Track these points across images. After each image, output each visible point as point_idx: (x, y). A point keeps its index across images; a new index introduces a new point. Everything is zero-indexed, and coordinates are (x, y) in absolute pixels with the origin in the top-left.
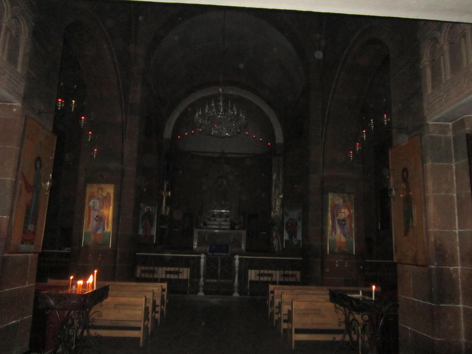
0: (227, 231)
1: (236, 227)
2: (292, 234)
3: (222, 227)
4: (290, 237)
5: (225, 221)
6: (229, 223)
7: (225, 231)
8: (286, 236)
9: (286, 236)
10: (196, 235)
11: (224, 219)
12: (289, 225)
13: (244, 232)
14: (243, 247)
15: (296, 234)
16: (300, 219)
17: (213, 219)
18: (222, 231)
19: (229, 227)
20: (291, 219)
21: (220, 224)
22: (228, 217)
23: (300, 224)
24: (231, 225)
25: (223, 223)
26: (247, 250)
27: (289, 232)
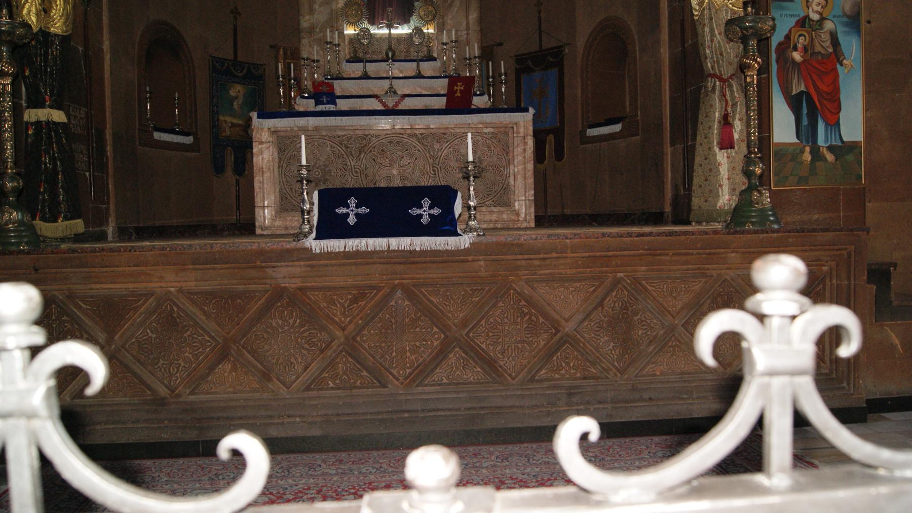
0: (433, 122)
1: (479, 101)
2: (816, 107)
3: (408, 104)
4: (805, 132)
5: (419, 76)
6: (441, 85)
7: (421, 122)
8: (784, 128)
9: (784, 128)
10: (264, 155)
11: (410, 68)
12: (797, 56)
13: (524, 121)
14: (523, 205)
15: (839, 109)
16: (853, 21)
17: (356, 69)
18: (401, 123)
19: (441, 103)
20: (803, 22)
21: (392, 91)
22: (430, 58)
23: (852, 47)
24: (450, 95)
25: (403, 87)
26: (541, 221)
27: (794, 103)
